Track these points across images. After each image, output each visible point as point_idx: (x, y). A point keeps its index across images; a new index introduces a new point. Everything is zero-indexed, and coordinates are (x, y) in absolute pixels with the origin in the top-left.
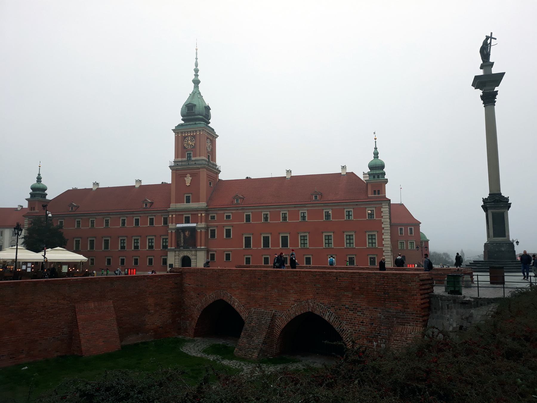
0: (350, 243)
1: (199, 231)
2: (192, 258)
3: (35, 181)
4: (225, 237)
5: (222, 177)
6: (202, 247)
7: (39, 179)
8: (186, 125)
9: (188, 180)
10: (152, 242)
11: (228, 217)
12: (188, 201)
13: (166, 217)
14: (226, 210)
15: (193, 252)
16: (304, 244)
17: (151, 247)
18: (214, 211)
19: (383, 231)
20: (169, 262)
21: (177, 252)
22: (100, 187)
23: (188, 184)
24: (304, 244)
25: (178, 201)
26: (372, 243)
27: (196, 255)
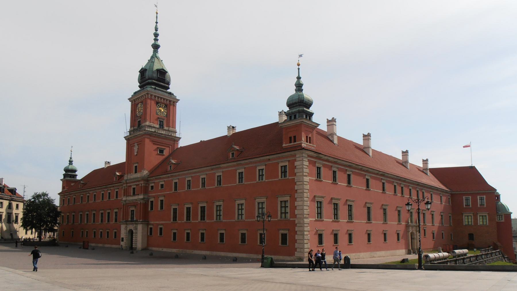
2: (134, 231)
3: (67, 164)
5: (182, 144)
11: (162, 185)
12: (136, 172)
14: (160, 178)
15: (135, 225)
17: (116, 220)
20: (122, 236)
22: (111, 164)
23: (136, 154)
25: (129, 172)
27: (136, 229)
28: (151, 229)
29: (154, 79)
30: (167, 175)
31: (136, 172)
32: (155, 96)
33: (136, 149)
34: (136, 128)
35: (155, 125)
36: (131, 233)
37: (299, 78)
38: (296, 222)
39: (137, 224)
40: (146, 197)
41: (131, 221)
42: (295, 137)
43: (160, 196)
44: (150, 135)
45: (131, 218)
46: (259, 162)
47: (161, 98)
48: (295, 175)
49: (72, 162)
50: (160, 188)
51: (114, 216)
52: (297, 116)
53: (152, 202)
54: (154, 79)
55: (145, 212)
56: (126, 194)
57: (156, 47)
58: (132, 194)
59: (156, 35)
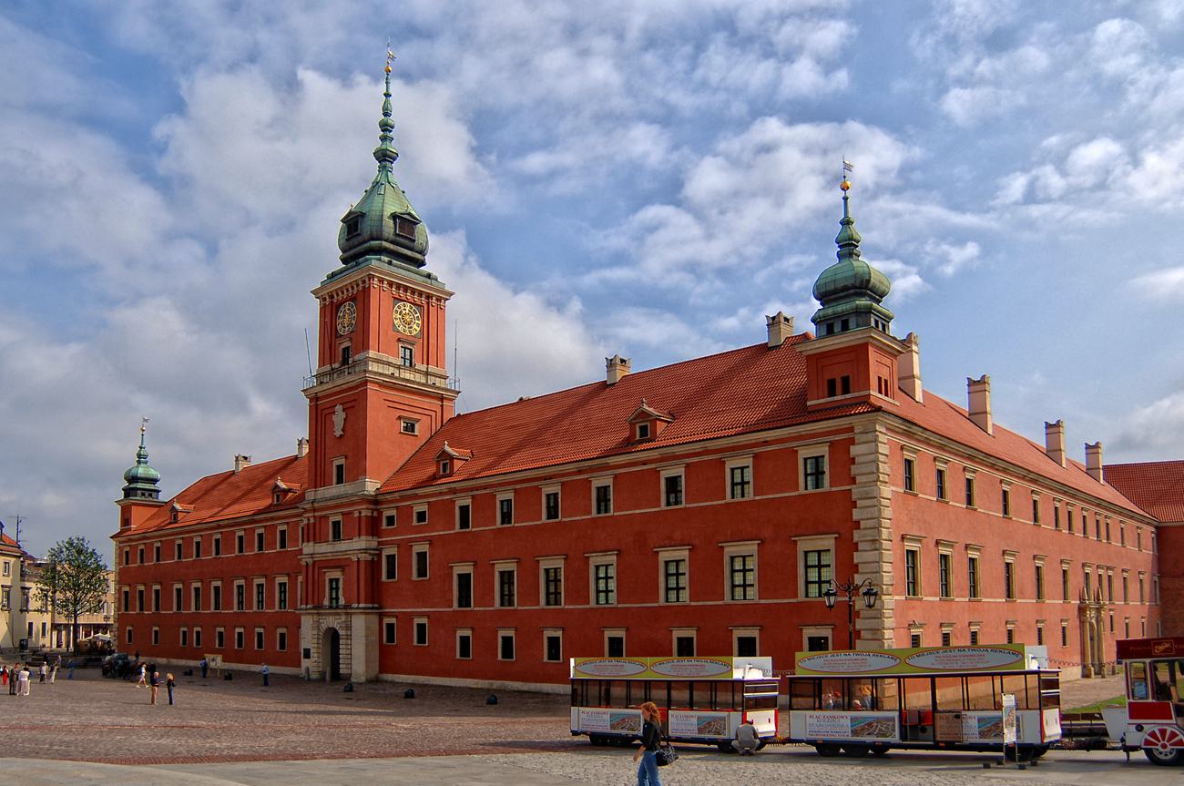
1: (355, 559)
2: (341, 632)
4: (415, 577)
6: (362, 605)
8: (342, 271)
9: (339, 417)
11: (421, 516)
12: (340, 481)
14: (417, 497)
15: (343, 618)
18: (392, 502)
19: (857, 536)
20: (304, 645)
21: (316, 618)
23: (338, 433)
26: (820, 582)
27: (349, 628)
28: (390, 626)
29: (377, 242)
31: (340, 481)
32: (391, 284)
34: (336, 365)
35: (391, 360)
36: (333, 638)
39: (351, 614)
40: (374, 544)
41: (331, 607)
42: (846, 381)
43: (416, 540)
44: (380, 385)
45: (331, 599)
46: (733, 449)
47: (406, 289)
48: (853, 481)
50: (415, 523)
51: (277, 595)
52: (852, 323)
53: (391, 558)
55: (374, 585)
56: (312, 534)
59: (386, 127)
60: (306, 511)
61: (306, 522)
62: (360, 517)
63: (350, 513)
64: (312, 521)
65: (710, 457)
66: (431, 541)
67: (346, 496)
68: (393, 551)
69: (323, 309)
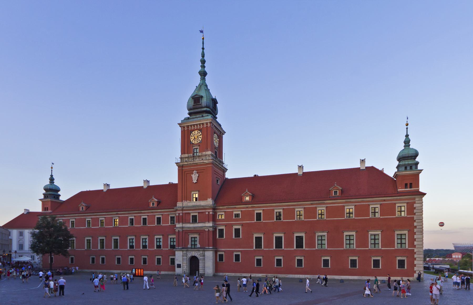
0: (375, 244)
1: (207, 230)
3: (48, 182)
7: (52, 180)
10: (160, 242)
11: (237, 215)
13: (173, 216)
14: (235, 208)
16: (322, 244)
23: (195, 181)
24: (322, 244)
26: (401, 244)
28: (221, 256)
30: (247, 206)
33: (195, 177)
37: (407, 136)
38: (415, 251)
45: (192, 245)
49: (54, 179)
50: (234, 217)
53: (221, 231)
54: (203, 107)
57: (203, 74)
58: (191, 222)
60: (177, 210)
61: (177, 215)
62: (208, 214)
63: (202, 213)
64: (181, 214)
65: (364, 203)
66: (242, 225)
67: (200, 206)
68: (223, 227)
69: (183, 133)
